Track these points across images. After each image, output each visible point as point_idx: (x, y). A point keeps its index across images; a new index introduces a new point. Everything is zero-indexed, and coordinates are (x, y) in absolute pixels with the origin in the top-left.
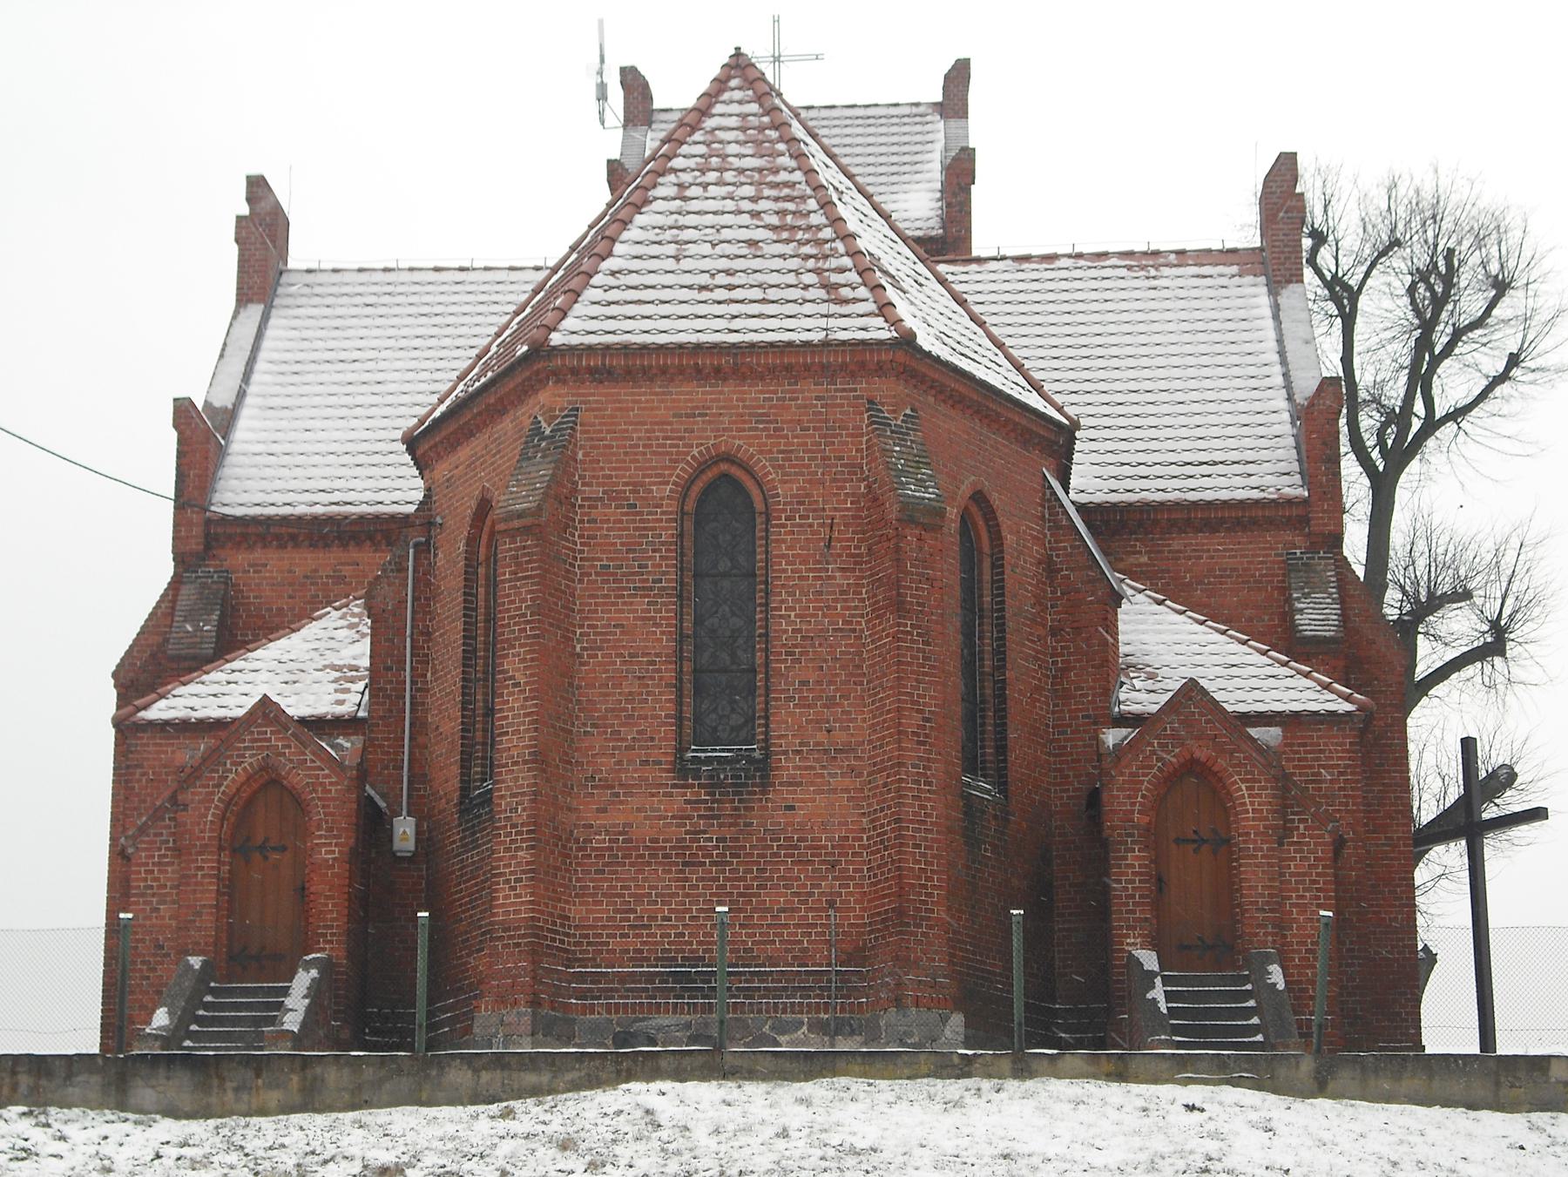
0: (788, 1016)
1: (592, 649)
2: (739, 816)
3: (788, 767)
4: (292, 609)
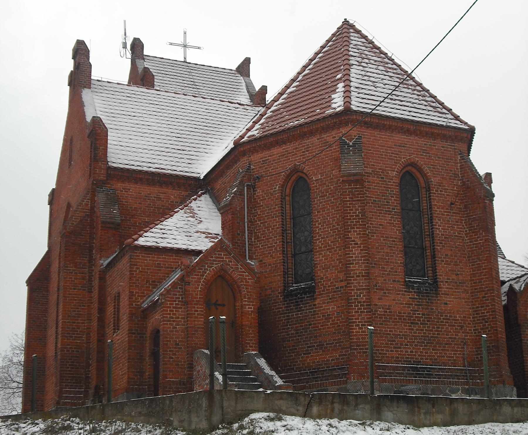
0: (454, 386)
1: (372, 233)
2: (429, 306)
3: (444, 287)
4: (141, 208)
